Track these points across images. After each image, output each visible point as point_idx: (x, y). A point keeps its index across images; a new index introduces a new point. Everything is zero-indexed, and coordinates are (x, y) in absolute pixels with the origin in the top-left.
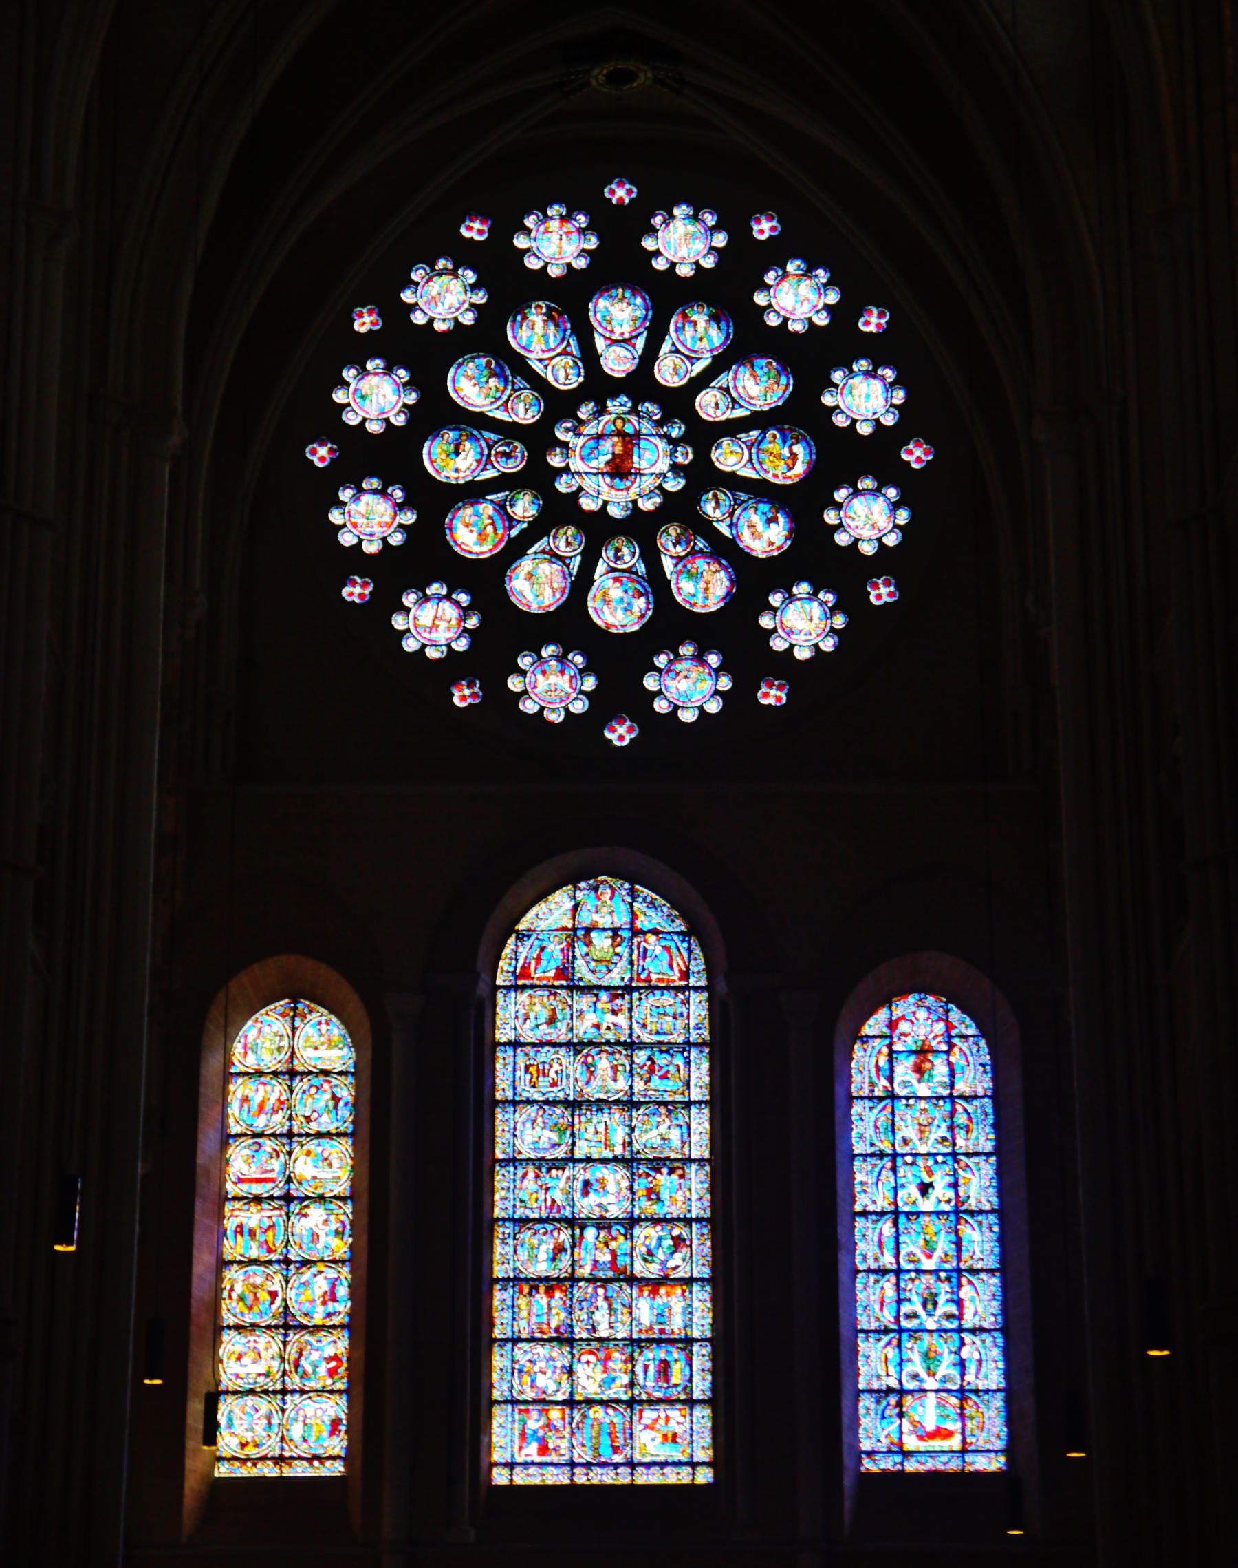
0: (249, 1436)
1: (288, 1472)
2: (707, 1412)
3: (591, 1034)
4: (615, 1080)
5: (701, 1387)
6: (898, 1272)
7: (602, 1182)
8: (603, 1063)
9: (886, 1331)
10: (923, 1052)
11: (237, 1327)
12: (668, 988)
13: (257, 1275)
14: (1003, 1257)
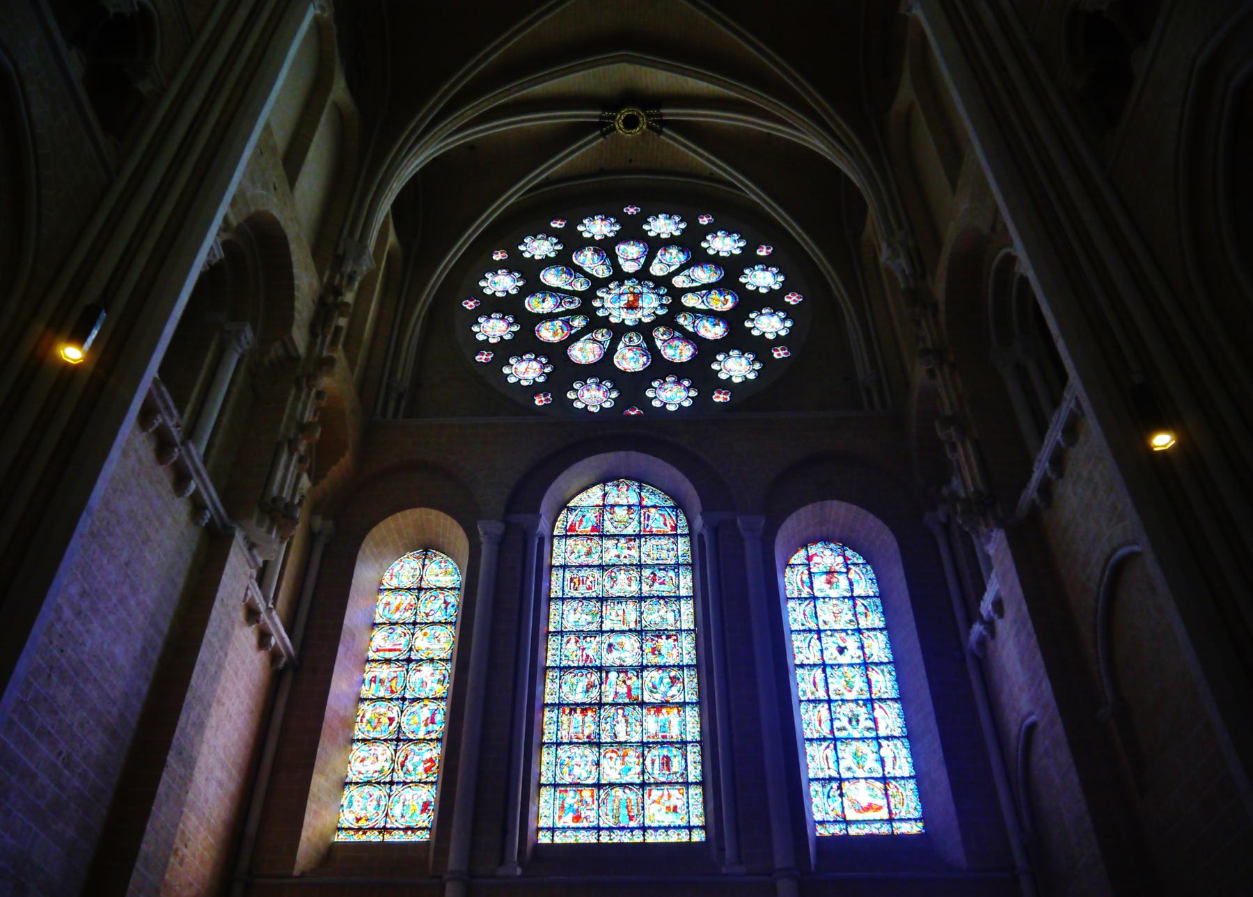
0: (362, 814)
1: (388, 838)
2: (699, 790)
3: (615, 561)
5: (694, 773)
6: (829, 701)
7: (621, 644)
8: (622, 577)
9: (825, 739)
10: (830, 573)
11: (364, 740)
12: (664, 535)
13: (382, 707)
14: (901, 690)
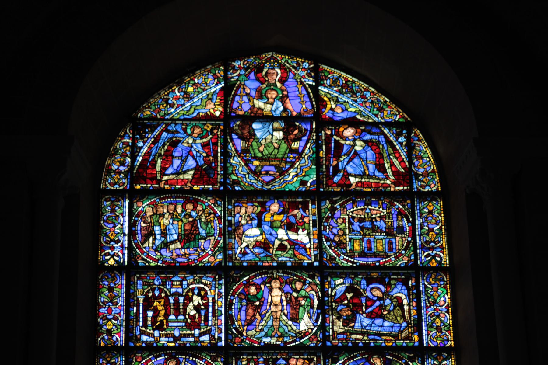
4: (296, 320)
